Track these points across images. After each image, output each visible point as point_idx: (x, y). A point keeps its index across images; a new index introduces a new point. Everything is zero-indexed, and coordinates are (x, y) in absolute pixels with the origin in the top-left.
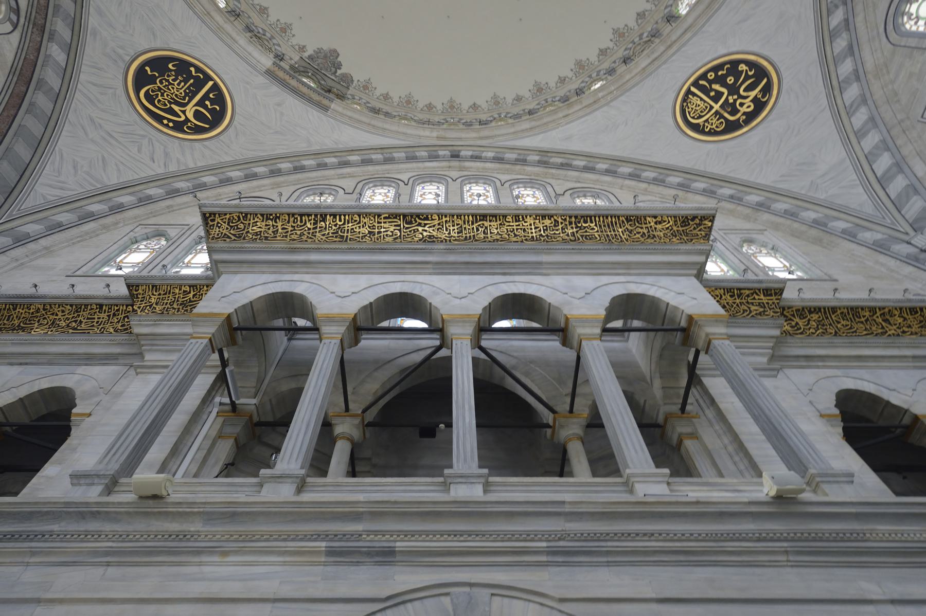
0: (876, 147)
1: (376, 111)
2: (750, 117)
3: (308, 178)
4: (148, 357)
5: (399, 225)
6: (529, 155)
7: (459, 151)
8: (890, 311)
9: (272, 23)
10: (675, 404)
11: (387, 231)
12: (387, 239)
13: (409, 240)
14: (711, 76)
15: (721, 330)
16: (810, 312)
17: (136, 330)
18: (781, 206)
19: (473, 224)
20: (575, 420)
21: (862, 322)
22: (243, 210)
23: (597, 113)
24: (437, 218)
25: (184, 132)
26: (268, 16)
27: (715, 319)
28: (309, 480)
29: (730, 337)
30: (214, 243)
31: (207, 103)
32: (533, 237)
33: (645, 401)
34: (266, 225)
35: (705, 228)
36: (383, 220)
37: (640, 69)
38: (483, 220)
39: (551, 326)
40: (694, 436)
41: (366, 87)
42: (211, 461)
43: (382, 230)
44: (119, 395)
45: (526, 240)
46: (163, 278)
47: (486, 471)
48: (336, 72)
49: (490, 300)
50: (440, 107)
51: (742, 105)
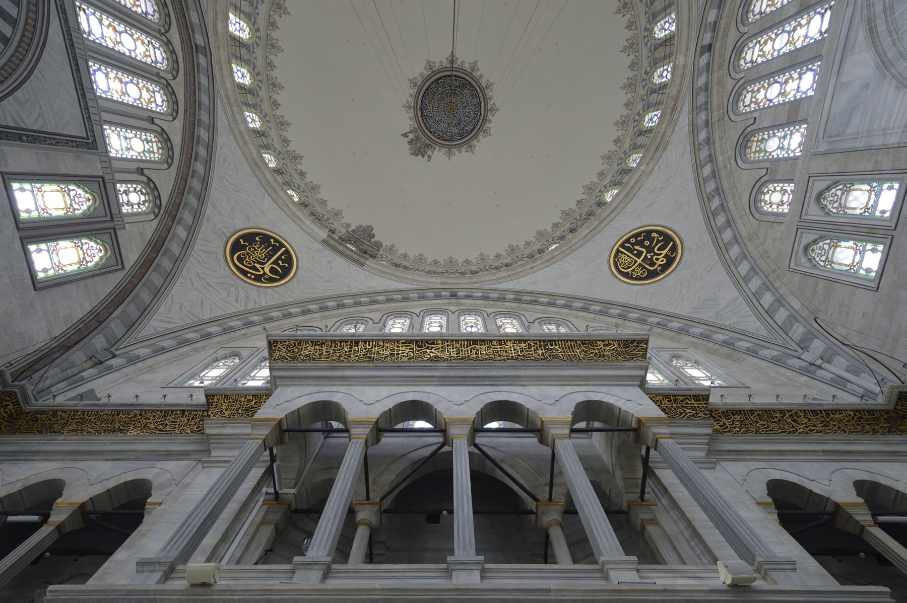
0: (759, 288)
1: (397, 266)
2: (665, 267)
3: (347, 312)
4: (213, 454)
5: (413, 349)
6: (507, 294)
7: (457, 292)
8: (796, 412)
10: (635, 493)
11: (403, 353)
12: (404, 359)
13: (420, 359)
14: (633, 240)
15: (664, 430)
16: (734, 414)
17: (208, 431)
18: (697, 330)
19: (467, 347)
20: (554, 507)
21: (775, 422)
22: (299, 339)
23: (555, 266)
24: (441, 342)
25: (262, 282)
27: (659, 422)
28: (334, 566)
29: (673, 435)
30: (274, 363)
31: (280, 262)
32: (512, 356)
33: (610, 490)
34: (314, 349)
35: (642, 349)
36: (400, 345)
37: (582, 236)
38: (475, 344)
39: (530, 427)
40: (654, 522)
41: (391, 249)
42: (254, 545)
43: (400, 352)
44: (187, 486)
45: (508, 359)
46: (233, 390)
47: (482, 558)
48: (371, 240)
49: (481, 406)
50: (442, 262)
51: (657, 259)
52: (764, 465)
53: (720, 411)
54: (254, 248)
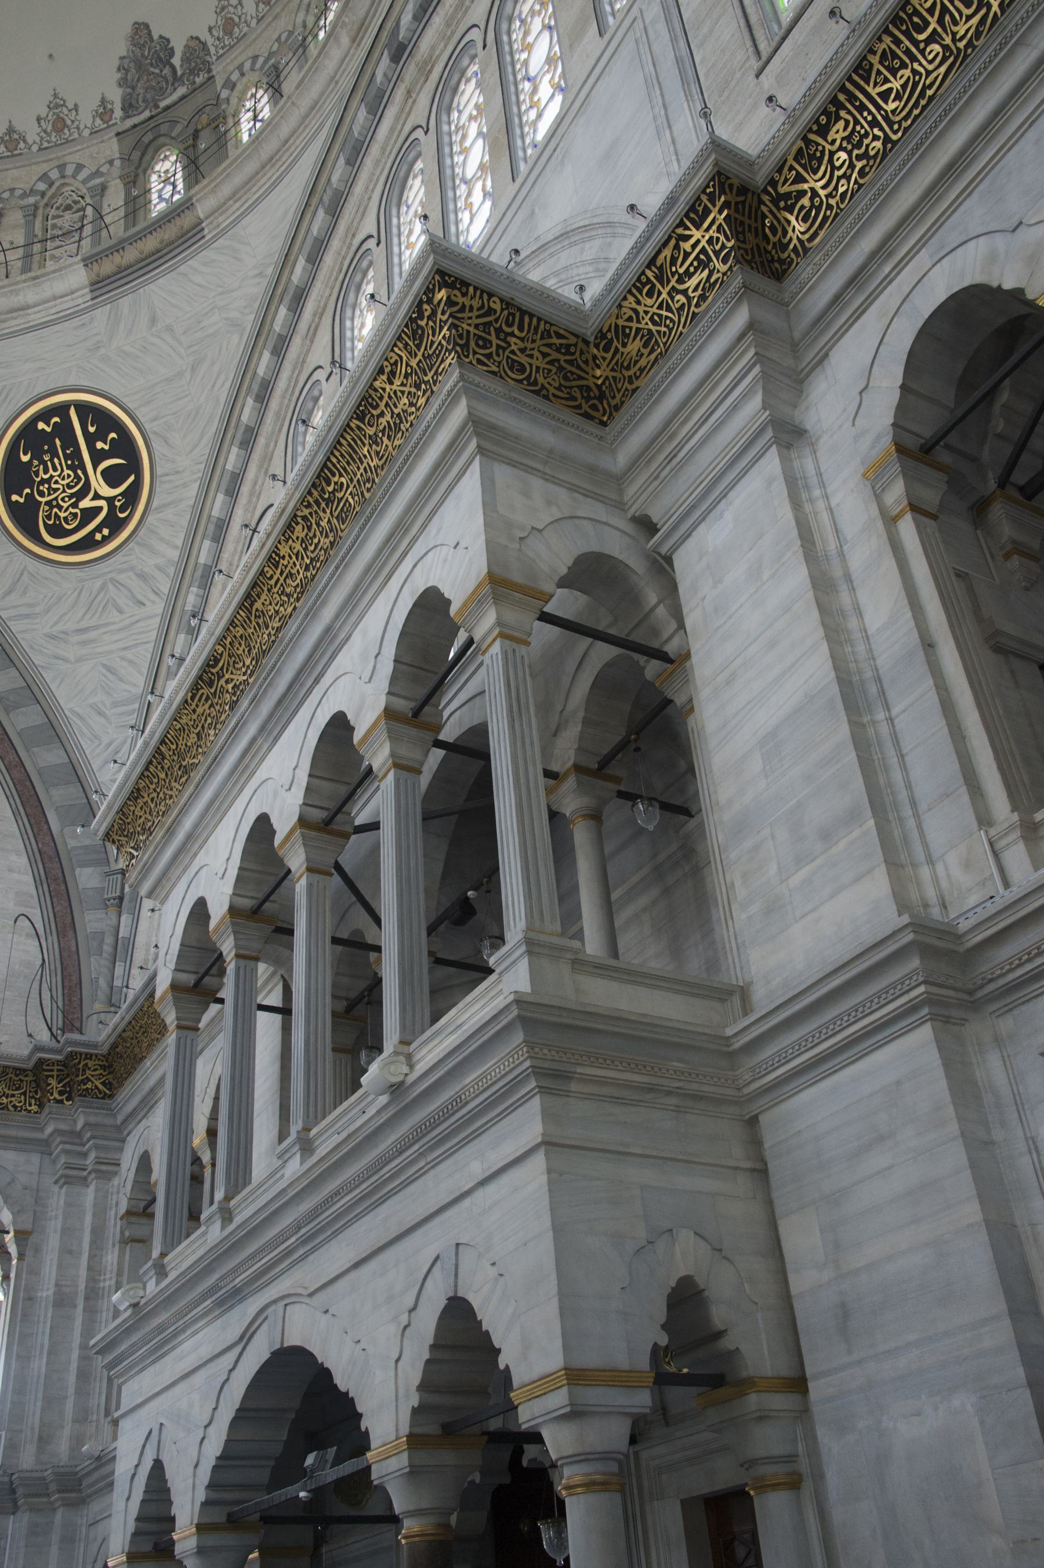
3: (284, 397)
9: (38, 140)
16: (823, 131)
19: (250, 621)
25: (126, 521)
26: (25, 141)
31: (100, 445)
52: (924, 259)
53: (791, 161)
54: (43, 482)
